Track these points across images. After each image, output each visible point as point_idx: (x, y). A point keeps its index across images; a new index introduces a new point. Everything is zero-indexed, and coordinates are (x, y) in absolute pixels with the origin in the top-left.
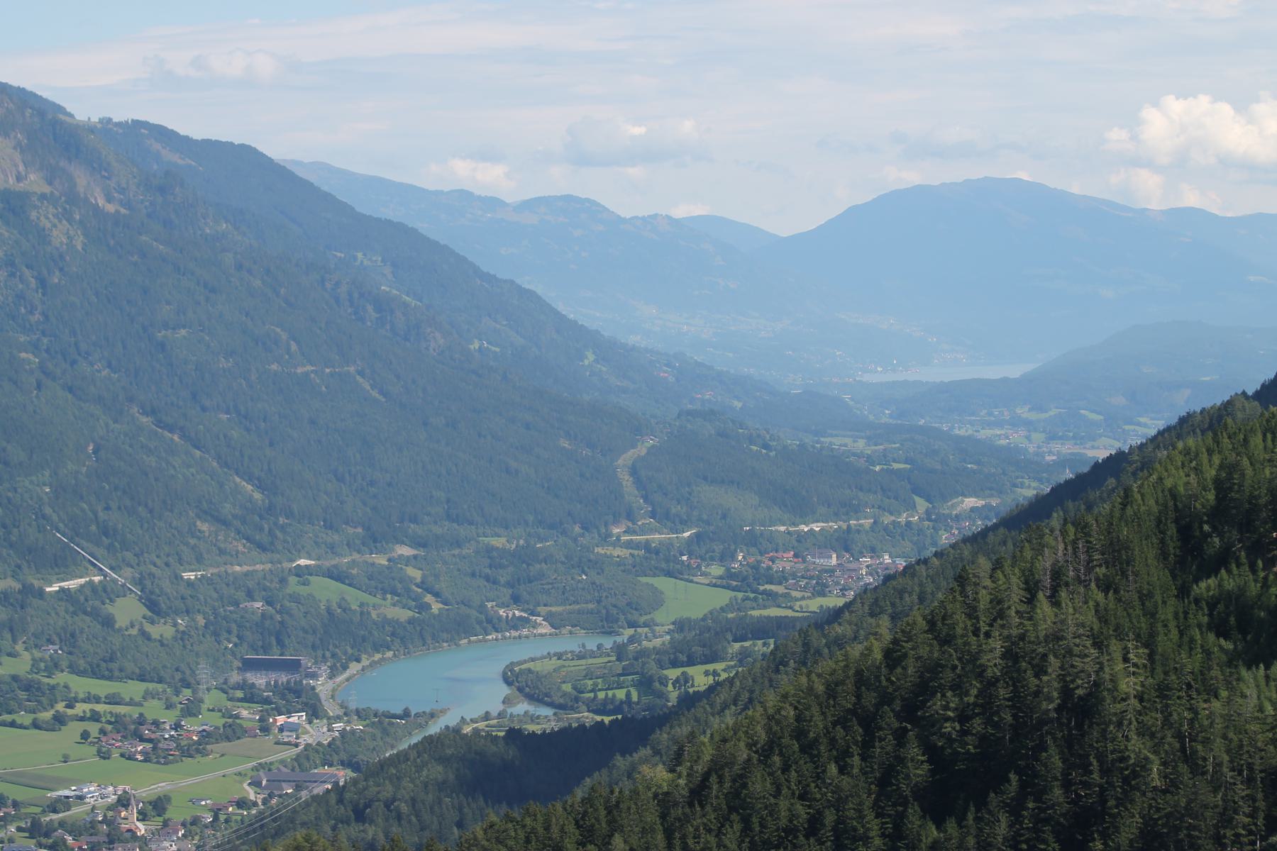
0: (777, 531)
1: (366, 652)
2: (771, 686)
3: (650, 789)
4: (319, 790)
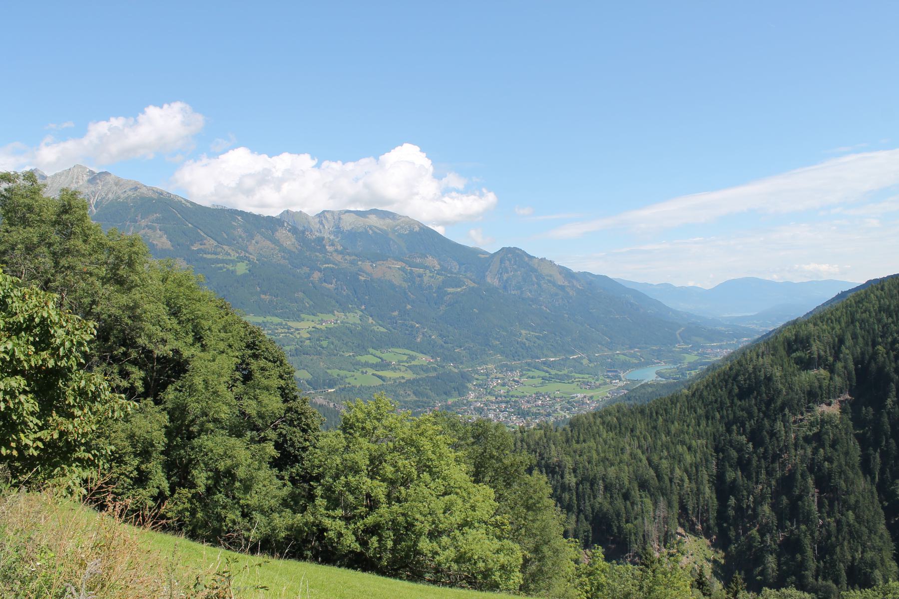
4: (621, 394)
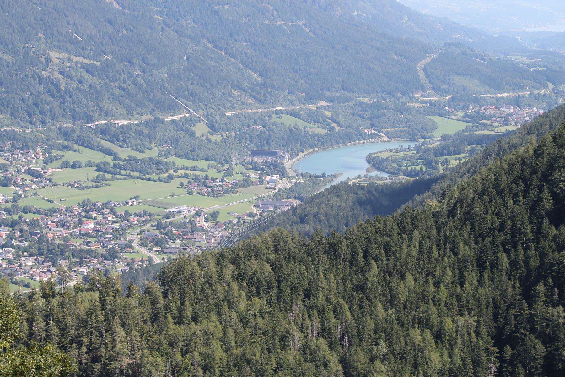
0: (487, 96)
1: (306, 148)
2: (484, 165)
3: (430, 210)
4: (285, 209)
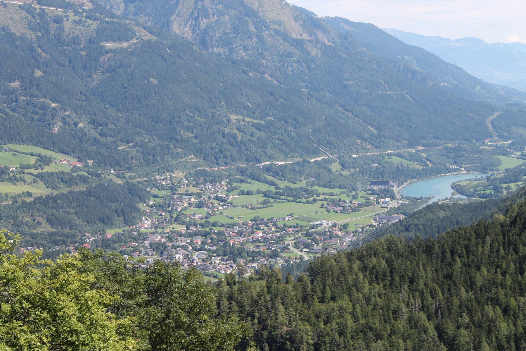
1: (409, 179)
4: (394, 222)
